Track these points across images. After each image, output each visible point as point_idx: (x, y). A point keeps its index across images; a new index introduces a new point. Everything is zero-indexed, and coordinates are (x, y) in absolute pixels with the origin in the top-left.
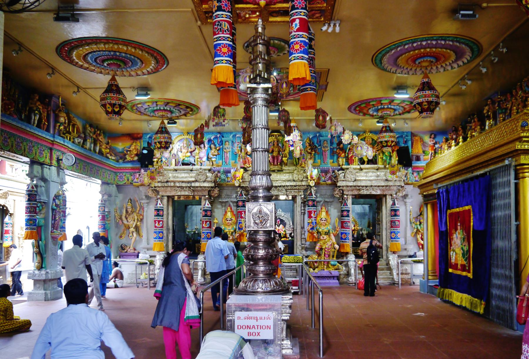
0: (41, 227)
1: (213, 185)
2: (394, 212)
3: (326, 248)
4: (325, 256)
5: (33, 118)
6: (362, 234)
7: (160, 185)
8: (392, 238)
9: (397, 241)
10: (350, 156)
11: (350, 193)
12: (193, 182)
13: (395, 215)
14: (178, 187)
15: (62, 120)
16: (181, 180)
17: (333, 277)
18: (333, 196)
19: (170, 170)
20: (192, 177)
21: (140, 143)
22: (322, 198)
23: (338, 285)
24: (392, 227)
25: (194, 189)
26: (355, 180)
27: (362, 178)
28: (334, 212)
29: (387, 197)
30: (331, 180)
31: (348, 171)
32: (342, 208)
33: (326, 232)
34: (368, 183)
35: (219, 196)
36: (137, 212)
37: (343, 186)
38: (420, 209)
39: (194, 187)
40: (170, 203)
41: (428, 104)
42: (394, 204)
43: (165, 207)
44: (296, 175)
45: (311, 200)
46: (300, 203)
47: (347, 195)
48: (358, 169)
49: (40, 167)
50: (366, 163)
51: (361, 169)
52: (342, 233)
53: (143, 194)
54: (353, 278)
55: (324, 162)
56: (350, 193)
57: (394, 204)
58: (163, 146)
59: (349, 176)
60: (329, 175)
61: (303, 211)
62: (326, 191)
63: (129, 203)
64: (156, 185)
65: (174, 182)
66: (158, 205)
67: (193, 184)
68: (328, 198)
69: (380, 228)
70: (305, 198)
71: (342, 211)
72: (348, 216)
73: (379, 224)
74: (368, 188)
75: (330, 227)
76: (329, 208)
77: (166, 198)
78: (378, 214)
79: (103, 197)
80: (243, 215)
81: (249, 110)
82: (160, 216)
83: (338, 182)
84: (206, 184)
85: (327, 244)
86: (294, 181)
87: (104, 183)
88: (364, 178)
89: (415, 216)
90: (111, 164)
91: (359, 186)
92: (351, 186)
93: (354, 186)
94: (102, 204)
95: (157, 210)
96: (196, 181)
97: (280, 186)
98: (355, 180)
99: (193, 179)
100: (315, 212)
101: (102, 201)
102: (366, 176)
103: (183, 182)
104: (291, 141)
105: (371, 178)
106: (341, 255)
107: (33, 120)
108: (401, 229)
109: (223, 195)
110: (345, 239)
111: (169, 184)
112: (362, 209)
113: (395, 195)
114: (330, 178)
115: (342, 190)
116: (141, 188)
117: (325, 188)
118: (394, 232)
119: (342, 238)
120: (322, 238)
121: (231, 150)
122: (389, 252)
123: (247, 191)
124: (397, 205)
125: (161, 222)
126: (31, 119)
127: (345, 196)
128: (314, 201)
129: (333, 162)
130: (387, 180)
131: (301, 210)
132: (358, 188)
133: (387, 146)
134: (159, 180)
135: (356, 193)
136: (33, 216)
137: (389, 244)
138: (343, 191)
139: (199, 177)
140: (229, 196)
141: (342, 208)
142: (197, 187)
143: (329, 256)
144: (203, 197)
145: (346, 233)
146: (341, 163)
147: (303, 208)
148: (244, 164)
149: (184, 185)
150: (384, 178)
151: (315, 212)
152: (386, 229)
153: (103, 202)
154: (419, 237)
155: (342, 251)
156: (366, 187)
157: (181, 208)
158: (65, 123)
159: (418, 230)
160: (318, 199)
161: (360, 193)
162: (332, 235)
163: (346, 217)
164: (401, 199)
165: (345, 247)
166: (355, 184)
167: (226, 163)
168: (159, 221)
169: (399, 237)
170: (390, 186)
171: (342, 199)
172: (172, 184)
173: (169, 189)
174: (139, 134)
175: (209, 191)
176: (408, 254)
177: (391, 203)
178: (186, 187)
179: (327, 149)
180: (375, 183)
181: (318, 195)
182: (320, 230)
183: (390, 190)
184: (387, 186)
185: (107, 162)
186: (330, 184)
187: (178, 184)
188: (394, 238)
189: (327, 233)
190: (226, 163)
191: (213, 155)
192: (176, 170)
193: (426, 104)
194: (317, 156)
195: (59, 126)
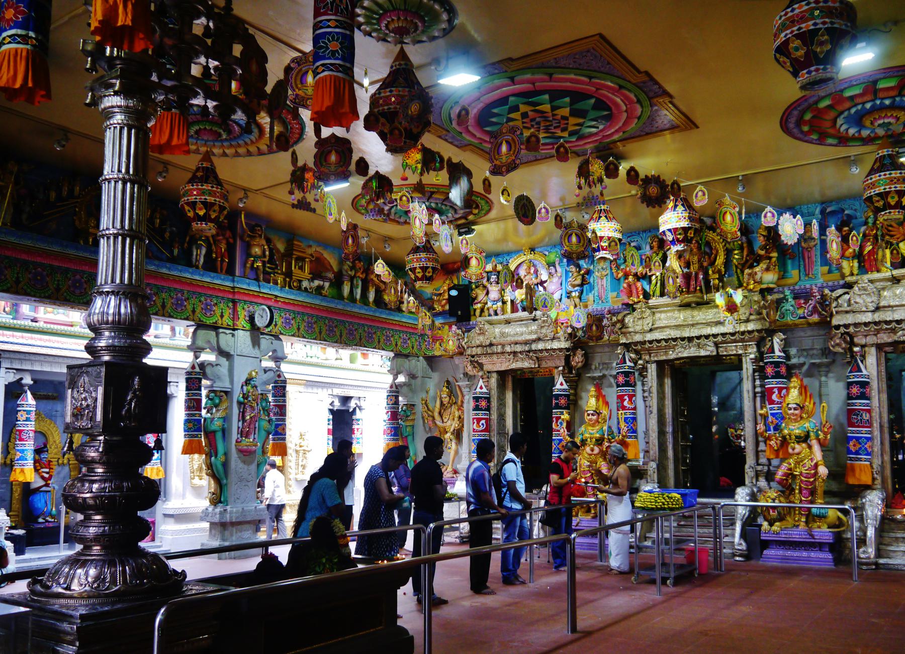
0: (214, 432)
3: (801, 473)
4: (800, 492)
5: (195, 253)
7: (479, 353)
10: (866, 252)
11: (871, 340)
12: (534, 341)
14: (509, 354)
15: (257, 250)
16: (513, 339)
17: (820, 546)
18: (826, 352)
19: (499, 322)
20: (531, 333)
21: (458, 278)
22: (806, 357)
23: (830, 566)
25: (538, 356)
26: (878, 309)
30: (820, 314)
31: (856, 288)
35: (587, 365)
36: (459, 403)
37: (846, 326)
39: (535, 351)
40: (510, 385)
41: (805, 43)
43: (494, 392)
45: (772, 363)
46: (750, 371)
48: (887, 280)
49: (214, 333)
53: (462, 371)
54: (871, 551)
55: (807, 275)
56: (871, 340)
58: (420, 275)
60: (812, 302)
61: (758, 390)
62: (811, 340)
63: (445, 389)
64: (475, 351)
65: (503, 346)
66: (478, 390)
67: (534, 347)
68: (816, 356)
70: (760, 357)
71: (850, 384)
75: (808, 425)
76: (823, 379)
77: (495, 375)
79: (395, 379)
80: (626, 403)
81: (326, 161)
82: (481, 410)
83: (831, 315)
84: (556, 345)
85: (804, 466)
87: (398, 355)
90: (404, 320)
91: (887, 322)
92: (866, 324)
93: (876, 323)
94: (391, 392)
95: (476, 399)
96: (539, 339)
97: (699, 338)
98: (878, 309)
99: (534, 337)
100: (780, 389)
101: (391, 387)
104: (668, 233)
106: (845, 489)
107: (194, 257)
109: (595, 363)
110: (857, 453)
111: (494, 349)
114: (815, 310)
115: (848, 333)
116: (457, 360)
117: (809, 333)
120: (790, 451)
121: (608, 271)
123: (637, 352)
125: (483, 422)
126: (192, 255)
127: (856, 349)
128: (777, 364)
129: (830, 272)
131: (754, 387)
132: (885, 326)
133: (887, 206)
134: (478, 342)
135: (885, 338)
136: (194, 415)
138: (852, 337)
139: (544, 331)
140: (607, 366)
141: (848, 377)
142: (541, 351)
143: (813, 493)
144: (556, 371)
145: (858, 439)
146: (847, 271)
147: (758, 382)
148: (629, 297)
149: (518, 348)
151: (780, 389)
153: (394, 389)
155: (852, 481)
157: (530, 392)
158: (265, 256)
160: (794, 361)
161: (896, 338)
162: (814, 443)
163: (857, 398)
166: (877, 317)
168: (479, 420)
172: (499, 349)
173: (495, 357)
174: (455, 263)
175: (567, 359)
179: (812, 243)
181: (793, 351)
182: (786, 432)
185: (391, 317)
186: (816, 324)
187: (508, 349)
189: (804, 439)
191: (574, 286)
192: (508, 322)
193: (797, 43)
194: (789, 262)
195: (253, 262)
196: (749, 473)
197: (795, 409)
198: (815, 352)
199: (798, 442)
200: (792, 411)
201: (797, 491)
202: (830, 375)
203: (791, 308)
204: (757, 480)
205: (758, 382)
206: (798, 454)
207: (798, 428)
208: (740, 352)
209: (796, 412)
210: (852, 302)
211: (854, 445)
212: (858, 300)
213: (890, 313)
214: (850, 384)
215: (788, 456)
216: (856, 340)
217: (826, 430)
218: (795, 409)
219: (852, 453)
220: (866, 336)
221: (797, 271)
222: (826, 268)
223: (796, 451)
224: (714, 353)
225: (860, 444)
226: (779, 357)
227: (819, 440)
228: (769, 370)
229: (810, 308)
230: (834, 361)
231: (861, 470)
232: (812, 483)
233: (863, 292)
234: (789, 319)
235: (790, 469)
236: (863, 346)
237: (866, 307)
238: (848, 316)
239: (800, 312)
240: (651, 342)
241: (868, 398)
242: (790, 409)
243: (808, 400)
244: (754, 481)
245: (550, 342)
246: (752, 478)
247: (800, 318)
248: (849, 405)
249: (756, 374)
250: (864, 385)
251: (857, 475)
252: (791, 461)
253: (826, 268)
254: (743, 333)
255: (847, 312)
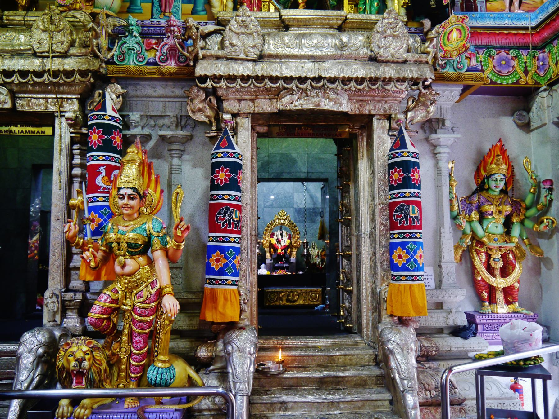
2: (402, 173)
6: (309, 255)
8: (393, 266)
9: (415, 279)
11: (246, 107)
13: (407, 183)
24: (393, 226)
26: (261, 57)
27: (287, 51)
28: (192, 180)
29: (375, 122)
32: (214, 156)
33: (130, 245)
34: (309, 69)
37: (217, 78)
38: (477, 172)
42: (399, 143)
44: (45, 36)
45: (99, 126)
46: (66, 140)
47: (235, 116)
50: (301, 5)
51: (284, 26)
52: (210, 250)
55: (163, 12)
57: (399, 143)
59: (241, 42)
60: (169, 41)
61: (77, 171)
62: (160, 99)
69: (349, 235)
72: (234, 185)
73: (347, 224)
74: (307, 85)
75: (153, 225)
76: (176, 161)
78: (345, 189)
83: (196, 60)
86: (35, 55)
88: (296, 51)
89: (463, 194)
92: (245, 79)
100: (110, 170)
102: (301, 46)
105: (317, 52)
108: (426, 234)
110: (221, 272)
112: (309, 200)
113: (401, 117)
118: (403, 245)
119: (209, 270)
120: (118, 269)
122: (386, 319)
124: (410, 148)
127: (227, 117)
128: (107, 129)
130: (373, 59)
131: (71, 167)
132: (269, 84)
135: (266, 106)
137: (381, 288)
138: (220, 100)
141: (214, 156)
145: (223, 250)
150: (365, 52)
152: (371, 235)
154: (479, 261)
155: (210, 316)
156: (302, 80)
159: (474, 236)
163: (226, 187)
164: (421, 135)
165: (221, 301)
166: (260, 69)
169: (420, 261)
170: (387, 81)
171: (219, 129)
176: (451, 323)
177: (389, 143)
180: (331, 70)
181: (134, 117)
182: (112, 236)
183: (385, 97)
184: (373, 80)
186: (171, 74)
188: (404, 268)
189: (142, 248)
196: (50, 304)
197: (130, 197)
198: (166, 121)
199: (132, 255)
200: (125, 201)
201: (125, 338)
202: (186, 157)
203: (137, 47)
204: (64, 316)
205: (77, 160)
206: (130, 275)
207: (133, 230)
208: (52, 109)
209: (132, 203)
210: (227, 43)
211: (218, 260)
212: (235, 41)
213: (276, 66)
214: (215, 166)
215: (113, 278)
216: (225, 105)
217: (179, 233)
218: (130, 197)
219: (213, 272)
220: (240, 101)
221: (148, 5)
222: (191, 6)
223: (128, 269)
224: (8, 106)
225: (226, 257)
226: (112, 118)
227: (166, 251)
228: (95, 137)
229: (165, 50)
230: (190, 138)
231: (226, 299)
232: (150, 324)
233: (243, 30)
234: (131, 63)
235: (115, 301)
236: (235, 116)
238: (219, 63)
239: (150, 56)
241: (240, 191)
242: (122, 197)
243: (153, 185)
244: (58, 319)
246: (55, 313)
247: (148, 63)
248: (213, 197)
249: (75, 147)
250: (236, 168)
251: (220, 309)
252: (118, 287)
253: (191, 6)
254: (56, 74)
255: (218, 58)
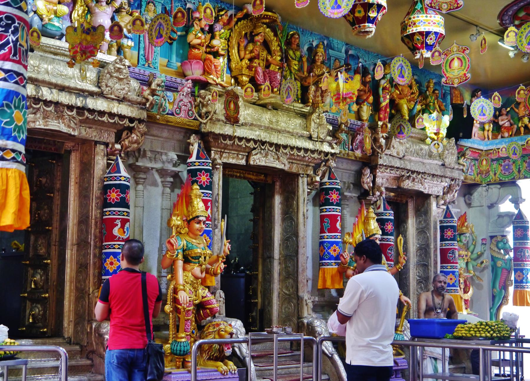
1: (144, 115)
12: (92, 94)
14: (47, 103)
39: (92, 111)
67: (91, 103)
86: (310, 138)
97: (285, 147)
103: (62, 89)
142: (102, 113)
149: (65, 98)
167: (147, 60)
178: (70, 108)
190: (147, 60)
237: (398, 153)
240: (240, 139)
245: (116, 104)
